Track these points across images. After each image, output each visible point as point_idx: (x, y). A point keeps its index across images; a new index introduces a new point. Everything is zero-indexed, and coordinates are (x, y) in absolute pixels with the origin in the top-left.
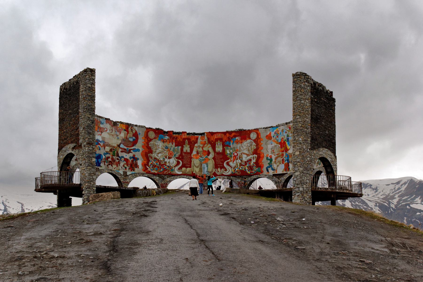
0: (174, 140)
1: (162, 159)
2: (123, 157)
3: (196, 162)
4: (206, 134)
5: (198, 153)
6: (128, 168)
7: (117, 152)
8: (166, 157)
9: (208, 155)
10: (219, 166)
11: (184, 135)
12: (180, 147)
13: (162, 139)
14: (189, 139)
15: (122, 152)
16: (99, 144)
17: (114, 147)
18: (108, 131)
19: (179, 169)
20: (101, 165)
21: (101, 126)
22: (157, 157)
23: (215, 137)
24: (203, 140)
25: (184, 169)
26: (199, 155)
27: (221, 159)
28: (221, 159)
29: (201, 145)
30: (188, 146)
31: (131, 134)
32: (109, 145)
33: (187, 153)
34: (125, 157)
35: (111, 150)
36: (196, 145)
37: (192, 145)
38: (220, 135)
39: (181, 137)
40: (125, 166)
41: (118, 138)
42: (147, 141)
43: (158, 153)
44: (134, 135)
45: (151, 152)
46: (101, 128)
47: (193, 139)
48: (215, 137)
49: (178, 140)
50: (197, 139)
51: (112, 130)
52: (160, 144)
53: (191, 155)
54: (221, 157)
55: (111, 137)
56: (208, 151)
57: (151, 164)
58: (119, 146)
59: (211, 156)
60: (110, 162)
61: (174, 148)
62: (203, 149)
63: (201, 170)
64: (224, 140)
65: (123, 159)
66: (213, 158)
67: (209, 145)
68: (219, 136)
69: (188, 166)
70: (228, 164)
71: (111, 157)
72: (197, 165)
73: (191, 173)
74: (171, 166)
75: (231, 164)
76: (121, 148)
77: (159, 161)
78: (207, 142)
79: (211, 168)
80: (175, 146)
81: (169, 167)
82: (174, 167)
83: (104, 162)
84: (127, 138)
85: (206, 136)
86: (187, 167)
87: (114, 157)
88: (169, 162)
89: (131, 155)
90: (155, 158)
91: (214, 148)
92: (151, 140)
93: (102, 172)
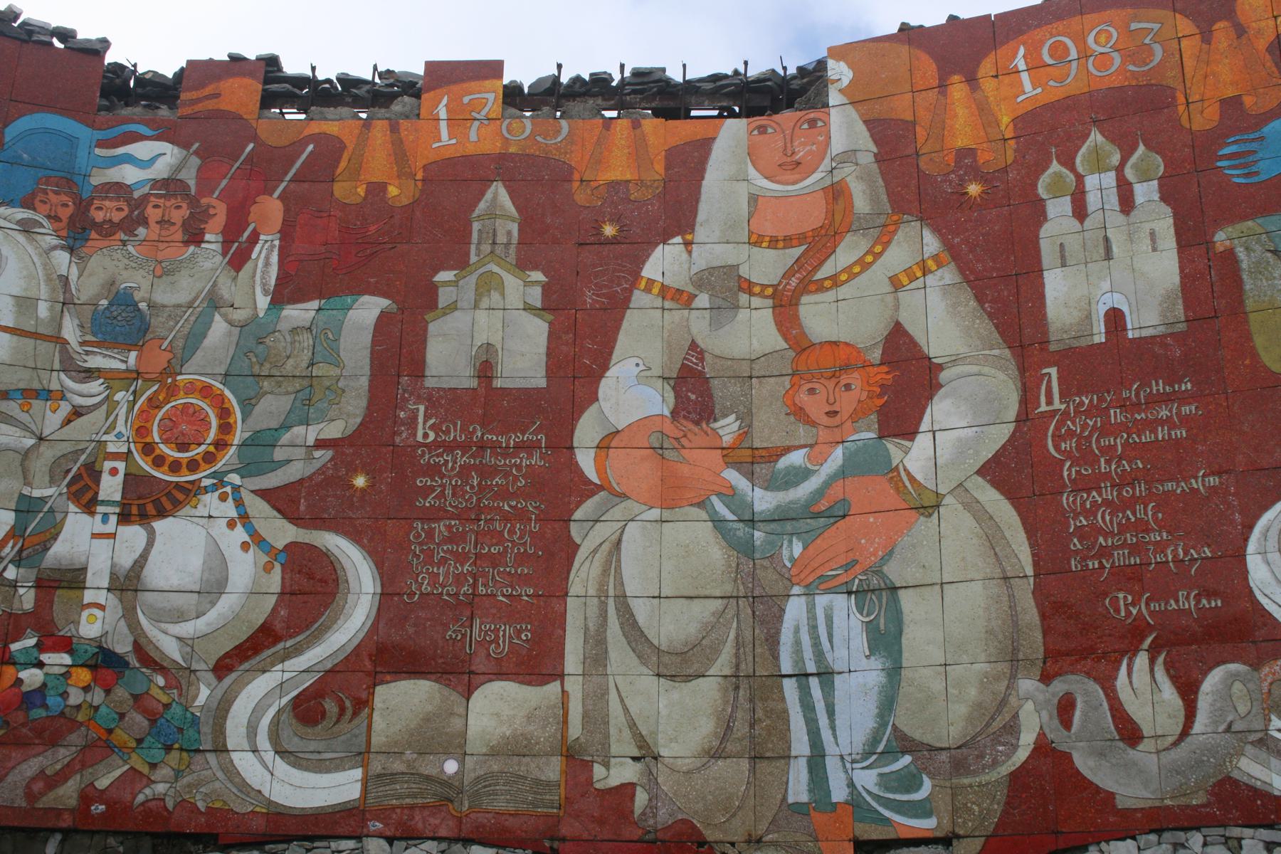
0: (271, 209)
4: (840, 72)
8: (84, 493)
9: (900, 419)
11: (459, 120)
13: (68, 182)
19: (306, 709)
24: (793, 167)
25: (403, 701)
26: (728, 428)
27: (1176, 459)
28: (1176, 459)
30: (523, 287)
33: (486, 401)
36: (664, 262)
39: (400, 155)
47: (618, 169)
49: (349, 191)
50: (689, 165)
53: (563, 445)
54: (1169, 422)
59: (958, 430)
61: (253, 334)
63: (754, 725)
66: (997, 471)
72: (672, 625)
74: (171, 649)
79: (974, 672)
80: (280, 298)
81: (104, 663)
82: (222, 668)
85: (855, 98)
88: (127, 584)
91: (1004, 279)
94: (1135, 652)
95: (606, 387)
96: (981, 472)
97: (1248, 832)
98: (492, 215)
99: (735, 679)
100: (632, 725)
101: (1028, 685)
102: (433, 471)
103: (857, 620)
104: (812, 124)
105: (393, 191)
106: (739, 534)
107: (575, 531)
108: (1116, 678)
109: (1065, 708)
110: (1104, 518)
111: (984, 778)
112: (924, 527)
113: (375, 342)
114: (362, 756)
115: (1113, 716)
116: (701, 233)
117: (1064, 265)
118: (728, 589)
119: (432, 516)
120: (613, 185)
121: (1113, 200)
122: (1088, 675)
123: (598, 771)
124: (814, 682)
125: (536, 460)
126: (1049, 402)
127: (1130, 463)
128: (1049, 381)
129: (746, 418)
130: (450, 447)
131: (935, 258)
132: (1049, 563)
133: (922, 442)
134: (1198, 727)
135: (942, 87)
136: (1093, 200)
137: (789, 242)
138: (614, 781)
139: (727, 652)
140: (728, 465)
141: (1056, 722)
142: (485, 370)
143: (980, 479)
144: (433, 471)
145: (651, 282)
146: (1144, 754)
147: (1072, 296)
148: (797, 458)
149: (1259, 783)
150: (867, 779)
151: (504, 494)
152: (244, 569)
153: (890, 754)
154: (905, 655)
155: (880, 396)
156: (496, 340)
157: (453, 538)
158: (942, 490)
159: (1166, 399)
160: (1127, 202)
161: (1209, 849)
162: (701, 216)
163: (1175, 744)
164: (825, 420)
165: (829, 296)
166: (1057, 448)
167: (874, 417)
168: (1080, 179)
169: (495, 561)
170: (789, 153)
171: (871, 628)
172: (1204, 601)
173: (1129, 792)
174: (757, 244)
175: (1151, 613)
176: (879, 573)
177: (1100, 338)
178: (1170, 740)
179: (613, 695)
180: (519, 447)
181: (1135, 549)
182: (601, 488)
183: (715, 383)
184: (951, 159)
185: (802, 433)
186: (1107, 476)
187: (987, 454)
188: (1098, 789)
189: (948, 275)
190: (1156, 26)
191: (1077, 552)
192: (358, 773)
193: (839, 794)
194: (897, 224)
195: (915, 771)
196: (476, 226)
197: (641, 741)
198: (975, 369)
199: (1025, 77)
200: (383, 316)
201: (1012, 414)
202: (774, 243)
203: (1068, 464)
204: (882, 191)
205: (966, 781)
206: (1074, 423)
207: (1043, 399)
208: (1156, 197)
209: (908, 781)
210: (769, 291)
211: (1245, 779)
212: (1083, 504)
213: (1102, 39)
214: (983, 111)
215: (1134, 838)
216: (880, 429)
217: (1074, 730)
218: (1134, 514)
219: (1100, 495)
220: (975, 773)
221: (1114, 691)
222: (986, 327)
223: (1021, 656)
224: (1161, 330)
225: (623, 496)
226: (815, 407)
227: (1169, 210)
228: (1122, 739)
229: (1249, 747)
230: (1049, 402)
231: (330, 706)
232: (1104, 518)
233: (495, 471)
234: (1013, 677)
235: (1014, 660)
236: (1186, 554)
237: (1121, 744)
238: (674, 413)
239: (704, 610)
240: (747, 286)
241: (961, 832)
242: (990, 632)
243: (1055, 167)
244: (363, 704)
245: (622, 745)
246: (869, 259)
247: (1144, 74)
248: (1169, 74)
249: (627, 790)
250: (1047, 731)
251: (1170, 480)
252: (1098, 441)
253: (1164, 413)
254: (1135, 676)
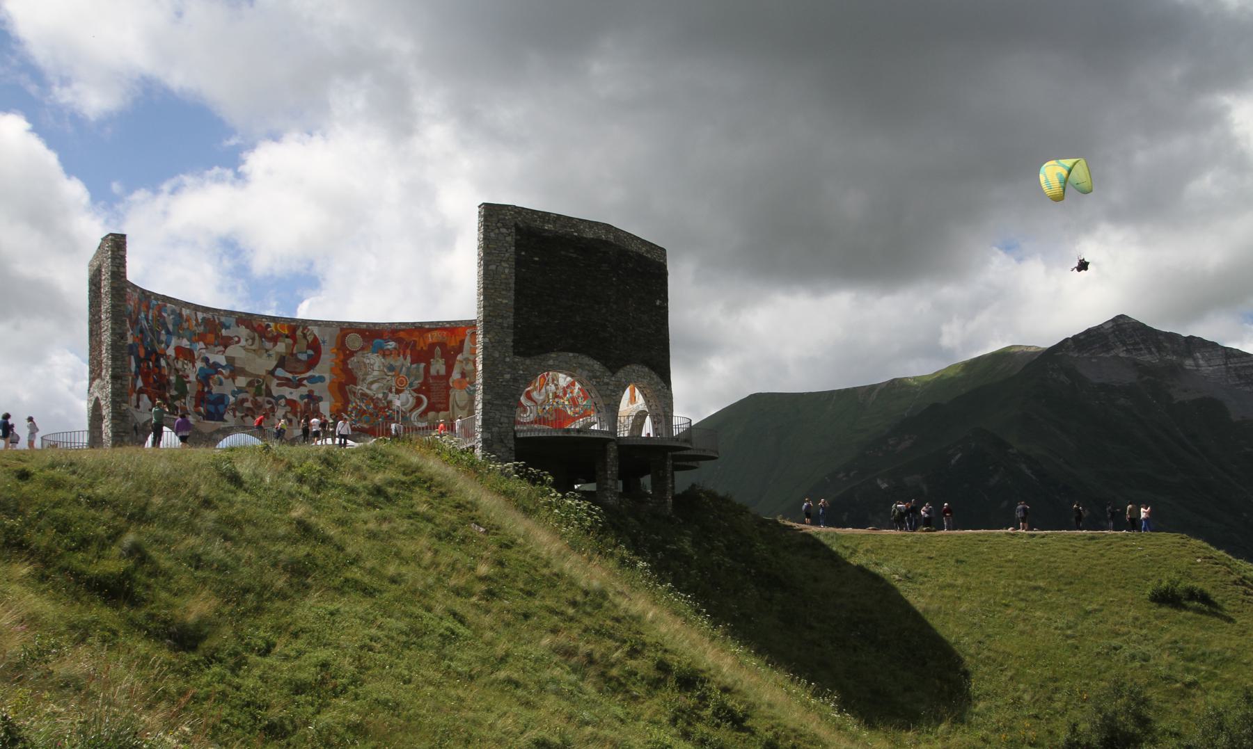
0: (408, 351)
1: (380, 396)
2: (282, 397)
6: (295, 420)
7: (267, 387)
12: (423, 365)
14: (443, 345)
15: (279, 385)
16: (217, 372)
17: (258, 376)
18: (243, 342)
20: (226, 417)
21: (224, 332)
22: (368, 392)
25: (431, 414)
30: (442, 361)
31: (303, 344)
32: (242, 372)
33: (438, 377)
34: (289, 397)
35: (250, 384)
36: (459, 357)
37: (450, 358)
40: (290, 416)
41: (269, 356)
42: (342, 357)
43: (372, 383)
44: (309, 347)
45: (353, 379)
46: (223, 338)
47: (453, 344)
49: (419, 348)
51: (253, 339)
52: (375, 361)
55: (251, 355)
57: (355, 408)
58: (272, 373)
60: (248, 409)
61: (408, 369)
65: (283, 402)
69: (443, 406)
70: (529, 397)
71: (250, 399)
72: (462, 404)
75: (535, 395)
76: (279, 378)
77: (372, 399)
82: (411, 411)
83: (234, 410)
84: (292, 354)
86: (438, 411)
87: (259, 399)
89: (303, 391)
90: (364, 395)
92: (352, 354)
93: (226, 432)
152: (411, 399)
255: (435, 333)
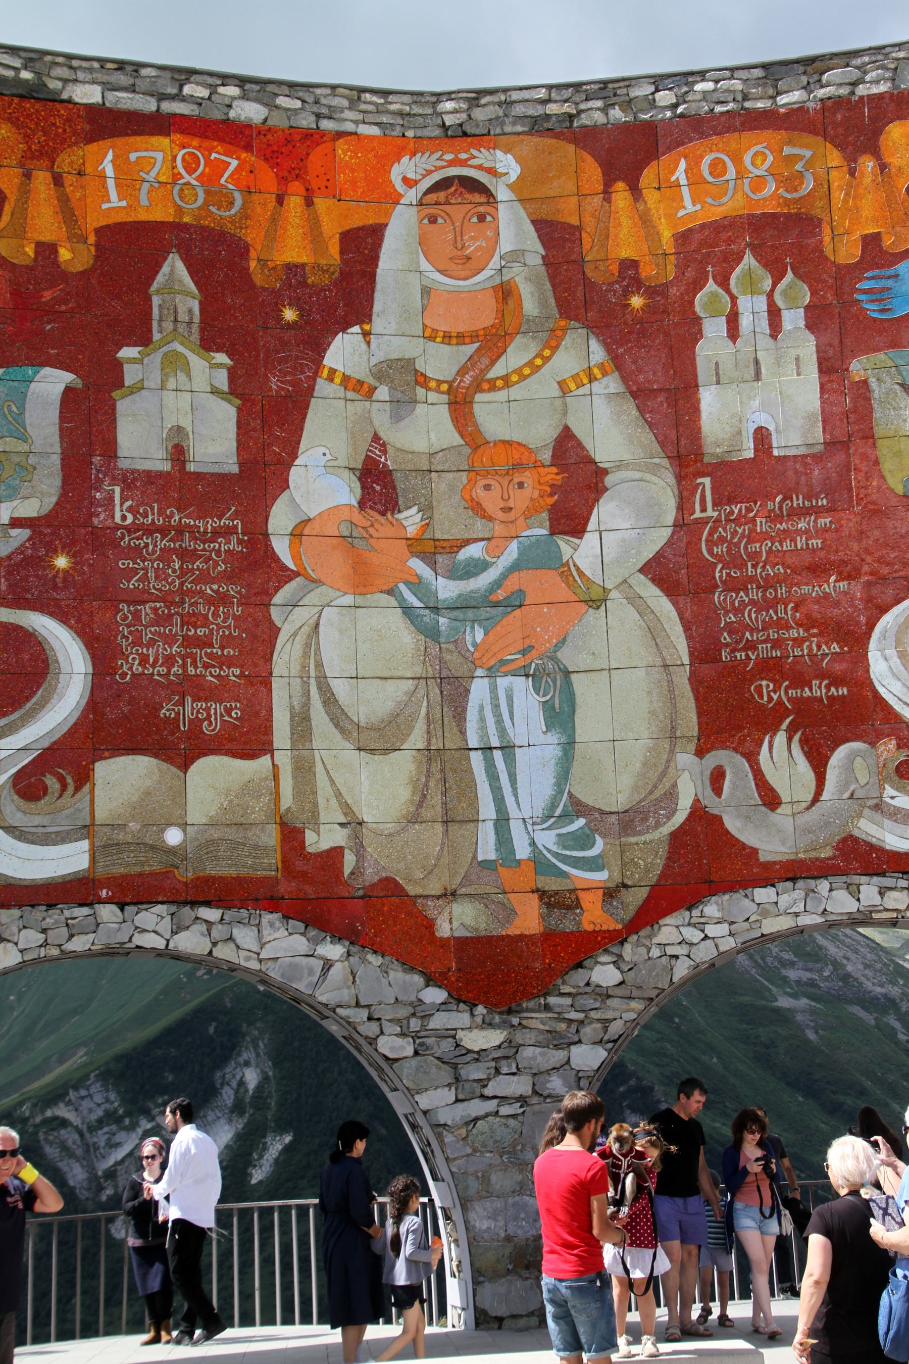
3: (343, 643)
5: (378, 484)
9: (570, 520)
10: (768, 692)
11: (128, 182)
12: (51, 383)
19: (28, 784)
23: (688, 193)
25: (123, 779)
26: (410, 519)
29: (441, 362)
30: (209, 370)
33: (179, 484)
36: (344, 352)
38: (758, 155)
39: (68, 213)
47: (293, 250)
48: (688, 193)
56: (567, 445)
62: (460, 407)
64: (847, 252)
66: (658, 570)
67: (580, 351)
68: (746, 177)
72: (371, 702)
73: (263, 854)
78: (532, 299)
86: (180, 749)
94: (775, 730)
95: (295, 475)
96: (641, 570)
97: (864, 879)
98: (169, 289)
99: (429, 755)
100: (338, 794)
101: (685, 758)
102: (136, 552)
103: (535, 700)
104: (482, 218)
105: (64, 254)
106: (424, 617)
107: (275, 614)
108: (759, 754)
109: (717, 778)
110: (750, 616)
111: (648, 837)
112: (593, 617)
113: (62, 419)
114: (87, 830)
115: (756, 785)
116: (378, 324)
117: (718, 383)
118: (418, 670)
119: (138, 599)
120: (292, 269)
121: (764, 325)
122: (736, 750)
123: (310, 837)
124: (497, 754)
125: (233, 545)
126: (704, 510)
127: (773, 567)
128: (703, 491)
129: (427, 509)
130: (150, 531)
131: (601, 366)
132: (704, 652)
133: (590, 539)
134: (826, 795)
135: (607, 194)
136: (745, 322)
137: (461, 339)
138: (325, 845)
139: (420, 726)
140: (414, 554)
141: (709, 791)
142: (178, 454)
143: (642, 577)
144: (136, 552)
145: (333, 371)
146: (782, 817)
147: (726, 415)
148: (474, 551)
149: (874, 840)
150: (547, 839)
151: (204, 577)
153: (566, 817)
154: (578, 731)
155: (551, 495)
156: (186, 423)
157: (162, 620)
158: (608, 585)
159: (803, 512)
160: (775, 326)
161: (834, 893)
162: (377, 307)
163: (808, 808)
164: (500, 515)
165: (502, 395)
166: (710, 552)
167: (545, 515)
168: (734, 299)
169: (205, 642)
170: (459, 246)
171: (548, 708)
172: (833, 689)
173: (770, 847)
174: (432, 338)
175: (789, 699)
176: (554, 659)
177: (750, 454)
178: (804, 805)
179: (319, 768)
180: (217, 533)
181: (776, 644)
182: (297, 574)
183: (397, 476)
184: (615, 268)
185: (480, 527)
186: (752, 579)
187: (648, 554)
188: (744, 846)
189: (612, 384)
190: (808, 154)
191: (727, 645)
192: (85, 844)
193: (522, 852)
194: (564, 330)
195: (588, 832)
196: (156, 301)
197: (347, 809)
198: (637, 475)
199: (685, 191)
200: (69, 391)
201: (670, 517)
202: (447, 338)
203: (719, 566)
204: (550, 294)
205: (633, 840)
206: (725, 530)
207: (697, 507)
208: (802, 323)
209: (583, 840)
210: (445, 387)
211: (863, 837)
212: (732, 603)
213: (759, 162)
214: (645, 221)
215: (773, 886)
216: (551, 527)
217: (723, 796)
218: (776, 613)
219: (747, 596)
220: (640, 833)
221: (758, 764)
222: (647, 437)
223: (678, 734)
224: (802, 451)
225: (317, 582)
226: (491, 502)
227: (812, 338)
228: (764, 805)
229: (866, 811)
230: (704, 510)
231: (51, 782)
232: (750, 616)
233: (193, 555)
234: (672, 751)
235: (673, 738)
236: (819, 647)
237: (763, 809)
238: (362, 504)
239: (397, 691)
240: (422, 380)
241: (629, 883)
242: (653, 713)
243: (711, 286)
244: (84, 777)
245: (331, 813)
246: (539, 362)
247: (796, 201)
248: (819, 204)
249: (336, 853)
250: (701, 798)
251: (807, 584)
252: (746, 548)
253: (802, 525)
254: (774, 751)
255: (157, 155)
